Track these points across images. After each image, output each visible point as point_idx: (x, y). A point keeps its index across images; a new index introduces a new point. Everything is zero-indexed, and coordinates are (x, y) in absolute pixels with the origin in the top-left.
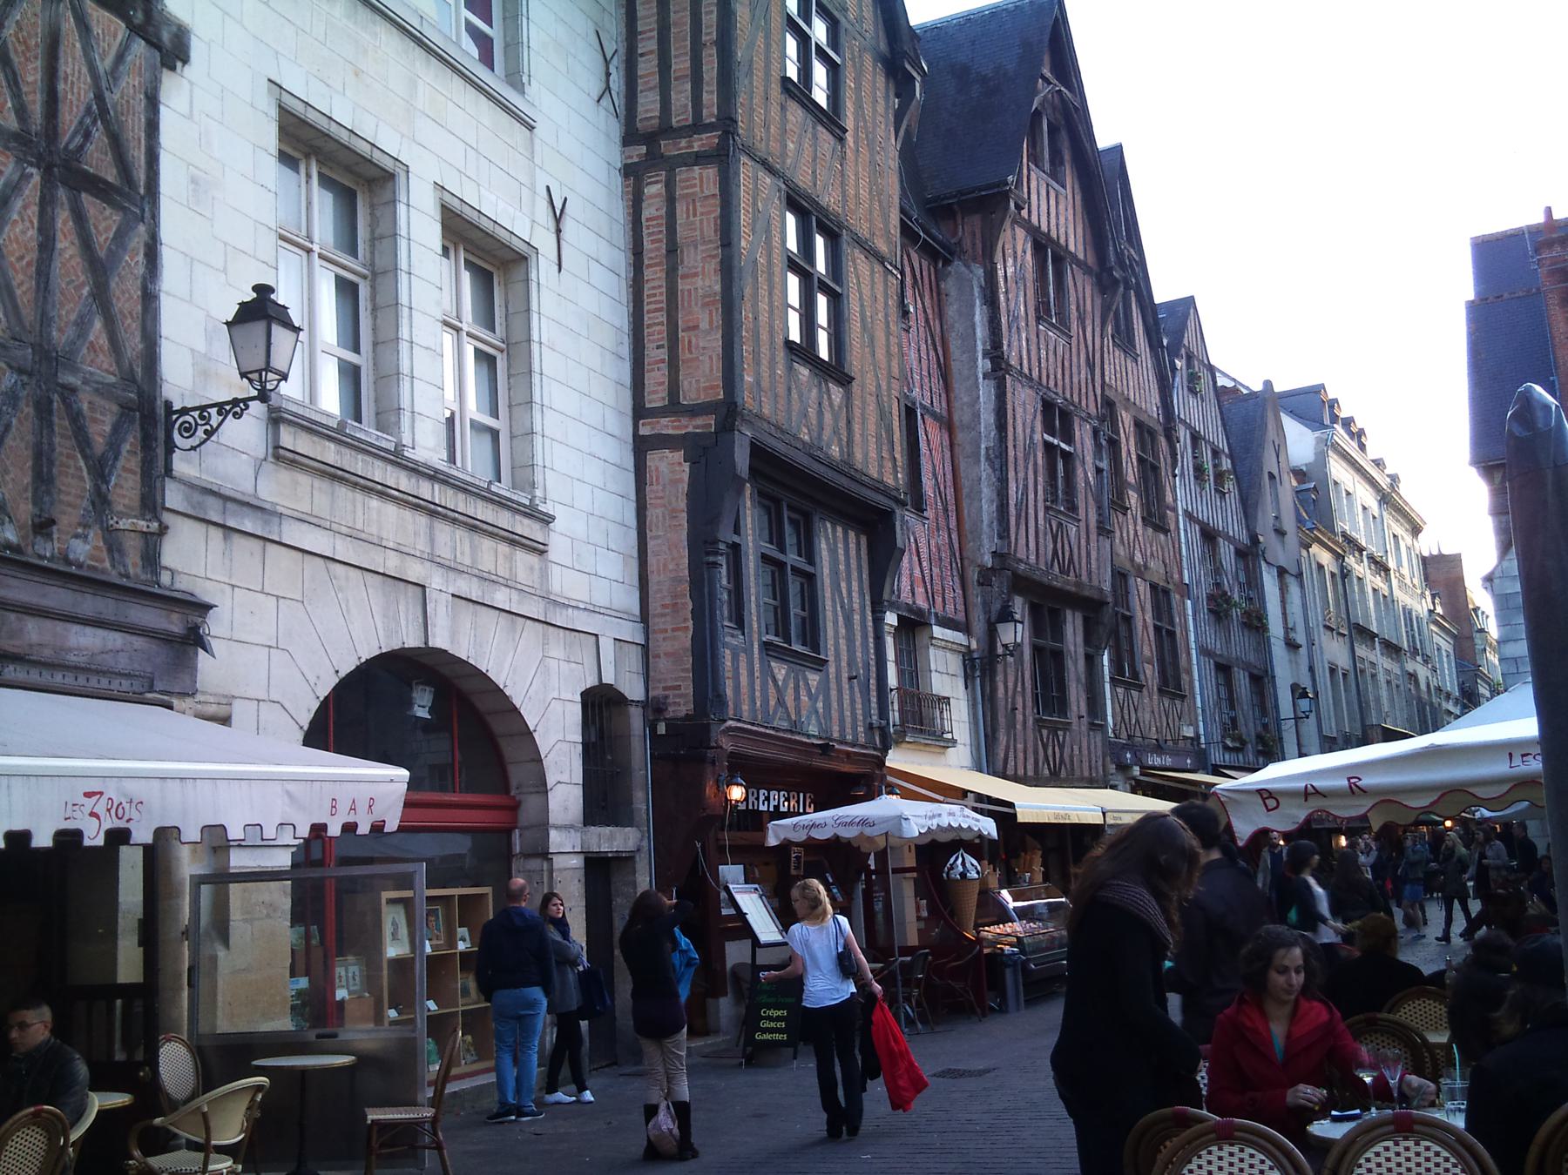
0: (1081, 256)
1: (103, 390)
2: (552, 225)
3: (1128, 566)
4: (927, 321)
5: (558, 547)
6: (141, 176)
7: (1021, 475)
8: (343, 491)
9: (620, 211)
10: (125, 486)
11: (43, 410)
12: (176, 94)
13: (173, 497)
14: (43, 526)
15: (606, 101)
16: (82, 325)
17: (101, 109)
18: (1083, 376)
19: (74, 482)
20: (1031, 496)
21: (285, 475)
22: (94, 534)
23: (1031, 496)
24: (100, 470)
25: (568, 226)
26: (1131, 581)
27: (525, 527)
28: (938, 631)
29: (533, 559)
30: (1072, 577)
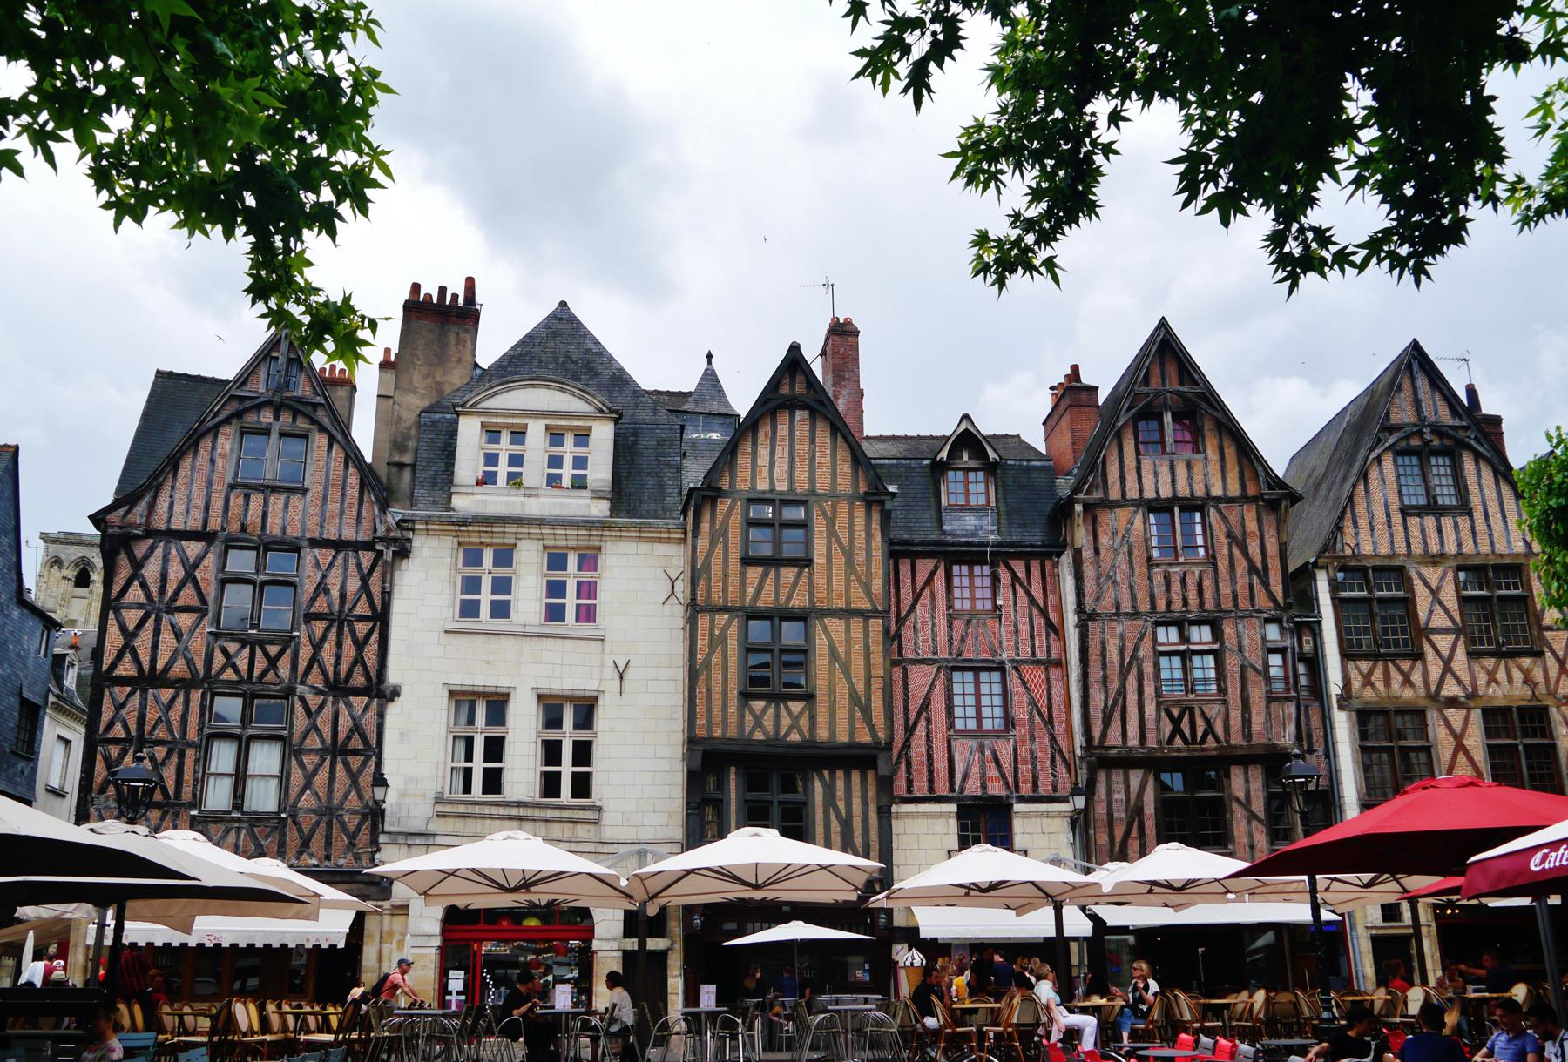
0: (1234, 490)
1: (354, 812)
2: (617, 676)
3: (1423, 703)
4: (1032, 601)
5: (607, 818)
6: (374, 743)
7: (1114, 686)
8: (469, 821)
9: (679, 649)
10: (364, 837)
11: (329, 825)
12: (393, 711)
13: (382, 838)
14: (328, 858)
15: (673, 600)
16: (346, 796)
17: (357, 727)
18: (1242, 581)
19: (341, 840)
20: (1132, 698)
21: (442, 820)
22: (349, 856)
23: (1132, 698)
24: (353, 837)
25: (628, 676)
26: (1432, 717)
27: (590, 815)
28: (1017, 807)
29: (592, 827)
30: (1211, 743)
